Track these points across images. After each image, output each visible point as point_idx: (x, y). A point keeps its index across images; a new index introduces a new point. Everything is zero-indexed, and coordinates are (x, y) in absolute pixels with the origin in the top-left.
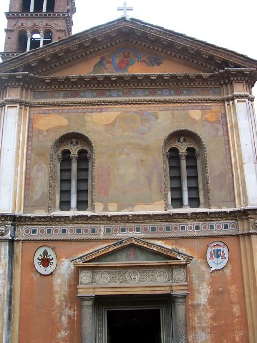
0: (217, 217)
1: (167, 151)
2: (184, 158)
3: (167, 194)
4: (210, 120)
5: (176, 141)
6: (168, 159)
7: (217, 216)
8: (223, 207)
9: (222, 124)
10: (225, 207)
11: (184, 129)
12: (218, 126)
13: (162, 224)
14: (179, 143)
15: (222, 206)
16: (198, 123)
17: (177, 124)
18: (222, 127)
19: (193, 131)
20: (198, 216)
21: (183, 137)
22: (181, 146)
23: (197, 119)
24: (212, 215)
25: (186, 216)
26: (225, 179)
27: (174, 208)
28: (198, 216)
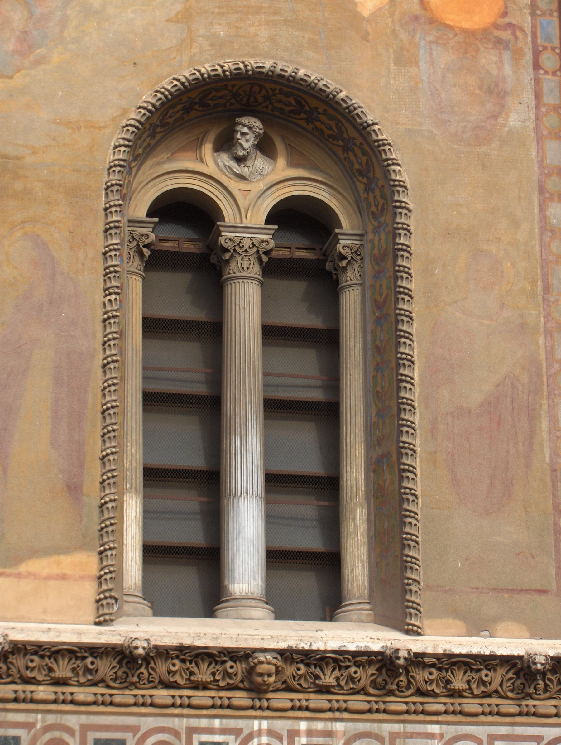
0: (458, 694)
1: (141, 212)
2: (255, 270)
3: (119, 508)
4: (450, 19)
5: (208, 149)
6: (137, 264)
7: (459, 683)
8: (501, 626)
9: (529, 57)
10: (513, 626)
11: (268, 64)
12: (508, 69)
13: (73, 721)
14: (225, 159)
15: (497, 619)
16: (365, 38)
17: (221, 32)
18: (527, 75)
19: (333, 86)
20: (329, 679)
21: (257, 124)
22: (234, 185)
23: (366, 14)
24: (421, 675)
25: (239, 668)
26: (532, 434)
27: (157, 613)
28: (329, 679)
